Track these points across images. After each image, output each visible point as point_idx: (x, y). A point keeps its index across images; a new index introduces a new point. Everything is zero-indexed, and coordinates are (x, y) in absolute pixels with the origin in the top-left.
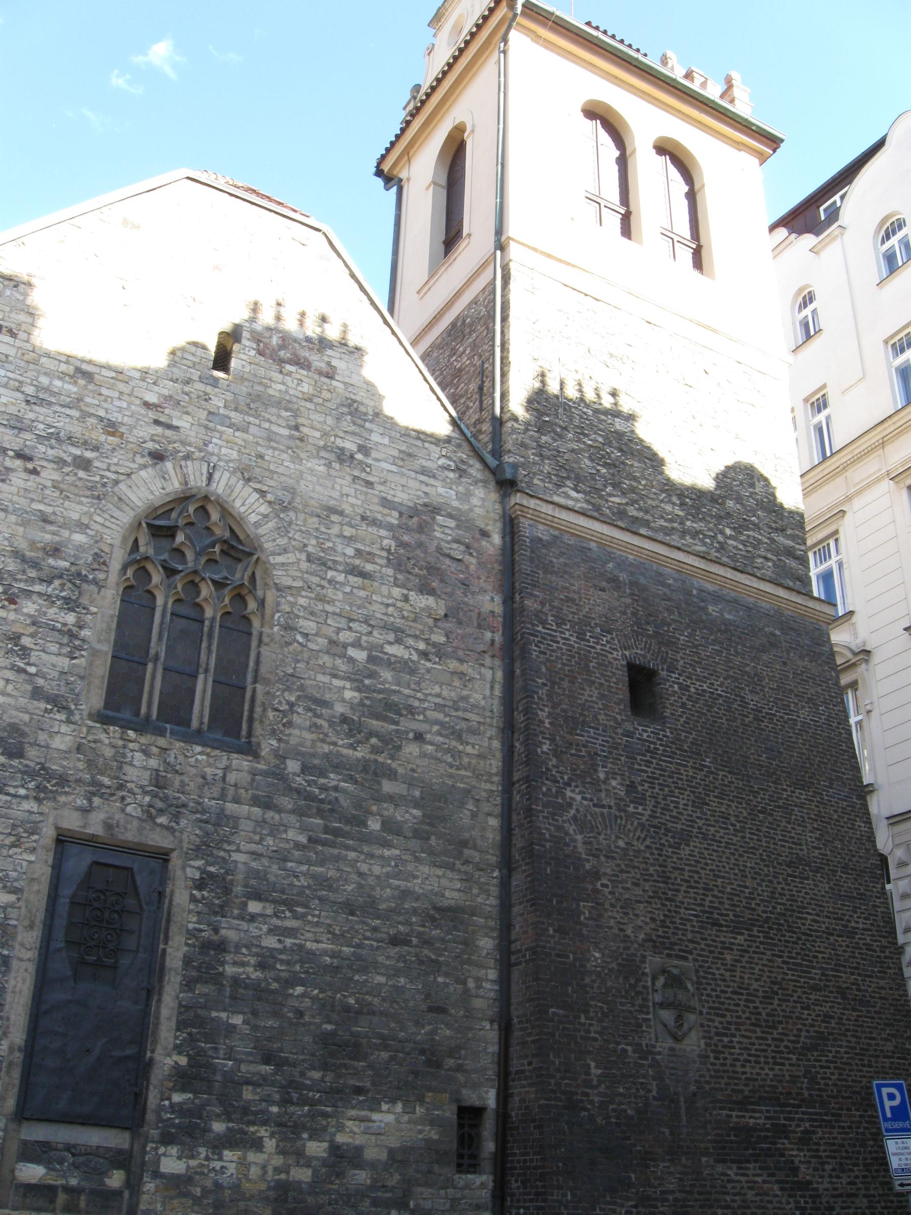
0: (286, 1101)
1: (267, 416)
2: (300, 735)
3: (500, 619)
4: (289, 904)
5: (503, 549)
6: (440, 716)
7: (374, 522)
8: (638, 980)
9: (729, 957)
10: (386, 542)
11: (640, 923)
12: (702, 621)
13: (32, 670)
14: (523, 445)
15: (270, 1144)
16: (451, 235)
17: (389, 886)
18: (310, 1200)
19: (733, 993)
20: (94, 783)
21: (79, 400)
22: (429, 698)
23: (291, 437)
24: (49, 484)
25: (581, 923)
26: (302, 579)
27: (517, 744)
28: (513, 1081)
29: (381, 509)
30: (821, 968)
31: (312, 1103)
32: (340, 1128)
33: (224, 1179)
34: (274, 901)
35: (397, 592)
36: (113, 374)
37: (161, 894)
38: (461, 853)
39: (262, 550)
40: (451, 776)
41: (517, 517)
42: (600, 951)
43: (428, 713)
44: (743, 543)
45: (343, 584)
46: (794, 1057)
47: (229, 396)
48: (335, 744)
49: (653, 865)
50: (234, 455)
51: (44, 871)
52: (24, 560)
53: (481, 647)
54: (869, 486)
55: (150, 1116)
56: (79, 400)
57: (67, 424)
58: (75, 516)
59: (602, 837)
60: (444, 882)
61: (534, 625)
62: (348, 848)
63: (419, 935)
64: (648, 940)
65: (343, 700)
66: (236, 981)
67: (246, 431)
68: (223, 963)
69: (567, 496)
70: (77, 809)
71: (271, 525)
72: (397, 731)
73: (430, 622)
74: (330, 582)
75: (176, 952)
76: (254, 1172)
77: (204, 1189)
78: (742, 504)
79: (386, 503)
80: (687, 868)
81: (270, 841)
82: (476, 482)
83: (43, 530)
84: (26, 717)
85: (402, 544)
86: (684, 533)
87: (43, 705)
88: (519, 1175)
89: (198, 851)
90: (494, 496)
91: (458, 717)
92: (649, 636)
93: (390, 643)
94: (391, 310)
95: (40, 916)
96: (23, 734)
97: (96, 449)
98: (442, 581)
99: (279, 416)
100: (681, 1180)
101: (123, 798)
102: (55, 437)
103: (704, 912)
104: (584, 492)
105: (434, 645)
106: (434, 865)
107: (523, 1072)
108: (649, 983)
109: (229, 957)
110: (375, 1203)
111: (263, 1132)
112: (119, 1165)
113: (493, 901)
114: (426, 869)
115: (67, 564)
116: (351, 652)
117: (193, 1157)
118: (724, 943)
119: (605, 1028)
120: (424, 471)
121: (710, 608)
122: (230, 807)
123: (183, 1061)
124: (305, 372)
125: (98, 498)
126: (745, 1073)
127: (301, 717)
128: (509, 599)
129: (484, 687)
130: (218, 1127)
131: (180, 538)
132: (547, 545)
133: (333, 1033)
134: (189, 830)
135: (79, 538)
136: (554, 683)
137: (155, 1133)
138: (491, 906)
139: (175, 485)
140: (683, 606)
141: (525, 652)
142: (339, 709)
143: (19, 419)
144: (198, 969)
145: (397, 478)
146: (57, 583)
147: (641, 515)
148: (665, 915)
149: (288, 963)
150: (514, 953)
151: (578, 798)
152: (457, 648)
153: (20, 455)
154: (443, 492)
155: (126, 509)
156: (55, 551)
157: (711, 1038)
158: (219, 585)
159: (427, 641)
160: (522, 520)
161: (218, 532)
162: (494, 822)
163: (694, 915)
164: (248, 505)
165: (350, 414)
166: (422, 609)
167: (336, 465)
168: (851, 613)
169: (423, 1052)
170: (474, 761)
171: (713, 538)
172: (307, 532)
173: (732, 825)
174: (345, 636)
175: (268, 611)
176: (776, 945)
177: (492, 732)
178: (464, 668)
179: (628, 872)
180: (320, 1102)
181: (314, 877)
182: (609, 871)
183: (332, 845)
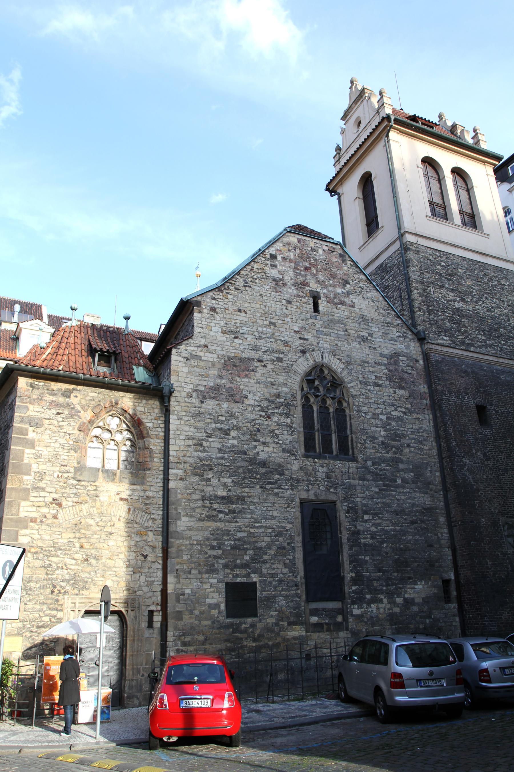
0: (387, 585)
2: (370, 452)
4: (377, 514)
6: (414, 436)
7: (379, 364)
8: (498, 528)
10: (384, 371)
13: (281, 442)
14: (424, 321)
15: (385, 601)
16: (372, 224)
17: (408, 503)
18: (400, 618)
20: (308, 480)
21: (273, 334)
23: (345, 335)
24: (271, 370)
32: (406, 592)
33: (373, 614)
34: (372, 514)
35: (391, 390)
37: (336, 517)
38: (429, 487)
39: (345, 382)
40: (421, 458)
42: (484, 518)
44: (509, 346)
45: (373, 391)
47: (321, 322)
48: (381, 453)
50: (328, 346)
51: (298, 515)
52: (269, 401)
53: (423, 407)
55: (347, 595)
56: (273, 334)
57: (272, 346)
58: (282, 381)
60: (425, 499)
62: (392, 491)
63: (420, 519)
64: (499, 512)
65: (381, 436)
66: (365, 544)
67: (330, 336)
68: (360, 539)
69: (443, 339)
70: (305, 491)
71: (346, 372)
73: (404, 400)
74: (369, 390)
75: (345, 536)
76: (382, 610)
77: (367, 619)
79: (382, 355)
81: (367, 492)
83: (273, 388)
84: (282, 460)
85: (390, 371)
86: (486, 346)
87: (287, 455)
89: (345, 499)
90: (418, 345)
92: (481, 393)
95: (301, 531)
96: (283, 466)
97: (283, 353)
99: (339, 327)
101: (318, 484)
102: (268, 351)
104: (448, 336)
105: (408, 409)
106: (421, 493)
109: (361, 536)
110: (421, 617)
111: (382, 597)
112: (340, 614)
113: (442, 503)
114: (418, 495)
116: (381, 417)
117: (362, 608)
120: (392, 339)
122: (352, 482)
123: (353, 575)
125: (288, 372)
128: (430, 387)
129: (426, 422)
130: (368, 596)
131: (317, 383)
132: (441, 362)
133: (398, 559)
134: (341, 494)
135: (285, 389)
137: (349, 601)
139: (311, 362)
141: (440, 407)
142: (381, 439)
143: (255, 346)
144: (352, 542)
145: (383, 344)
146: (281, 408)
149: (380, 535)
151: (468, 461)
153: (259, 361)
154: (400, 347)
156: (278, 396)
158: (333, 399)
159: (405, 408)
161: (328, 377)
162: (438, 474)
164: (337, 365)
167: (362, 343)
169: (428, 562)
171: (498, 346)
172: (358, 372)
174: (378, 411)
175: (351, 406)
177: (432, 439)
178: (419, 416)
180: (398, 584)
181: (383, 503)
183: (387, 490)
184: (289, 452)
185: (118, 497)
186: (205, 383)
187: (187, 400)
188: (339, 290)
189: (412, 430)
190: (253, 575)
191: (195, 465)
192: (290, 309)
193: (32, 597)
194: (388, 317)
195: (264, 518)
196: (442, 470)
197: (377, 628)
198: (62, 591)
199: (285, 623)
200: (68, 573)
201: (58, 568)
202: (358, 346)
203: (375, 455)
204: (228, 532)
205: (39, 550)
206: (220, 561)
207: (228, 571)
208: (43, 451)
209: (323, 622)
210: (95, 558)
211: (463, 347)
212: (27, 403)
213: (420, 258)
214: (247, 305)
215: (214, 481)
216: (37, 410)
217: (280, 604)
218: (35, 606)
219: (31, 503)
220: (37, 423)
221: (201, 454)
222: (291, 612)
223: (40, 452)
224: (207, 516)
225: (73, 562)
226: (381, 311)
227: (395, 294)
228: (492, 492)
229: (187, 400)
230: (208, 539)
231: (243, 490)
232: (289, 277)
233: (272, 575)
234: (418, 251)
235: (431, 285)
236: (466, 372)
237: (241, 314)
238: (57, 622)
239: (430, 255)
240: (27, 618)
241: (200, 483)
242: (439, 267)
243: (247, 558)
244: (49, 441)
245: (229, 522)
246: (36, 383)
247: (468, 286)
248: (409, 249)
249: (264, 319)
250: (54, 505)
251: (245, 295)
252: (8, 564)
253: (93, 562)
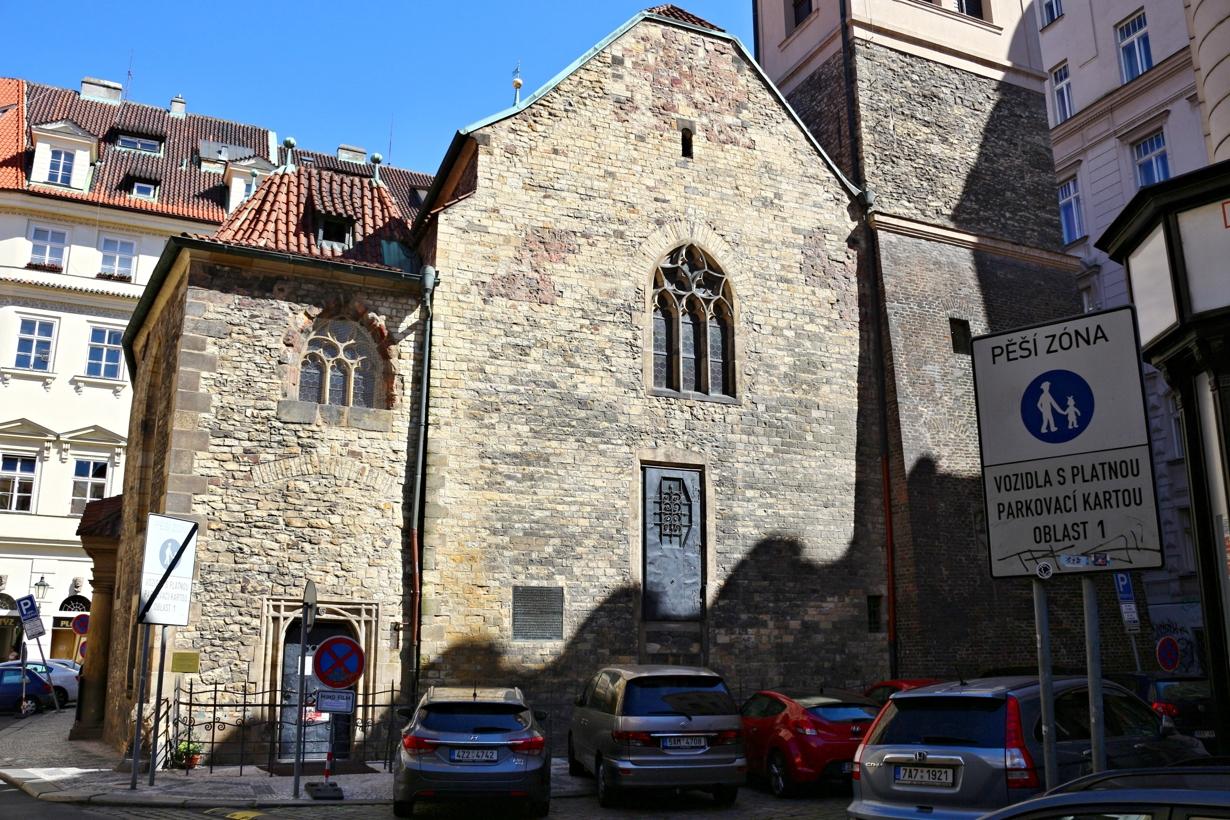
0: (777, 600)
1: (719, 183)
6: (840, 366)
8: (966, 518)
13: (613, 369)
15: (771, 624)
22: (834, 356)
24: (603, 251)
26: (753, 290)
27: (887, 379)
29: (793, 235)
31: (790, 600)
32: (806, 613)
35: (808, 289)
36: (627, 171)
43: (833, 365)
44: (1017, 221)
48: (783, 391)
54: (1100, 142)
58: (621, 270)
62: (795, 453)
67: (708, 196)
71: (731, 256)
72: (817, 379)
76: (764, 639)
78: (1016, 194)
79: (795, 230)
81: (753, 454)
83: (605, 281)
87: (623, 390)
91: (850, 365)
92: (962, 298)
93: (807, 323)
94: (757, 59)
104: (914, 202)
108: (973, 519)
109: (739, 523)
112: (696, 641)
113: (879, 476)
115: (622, 302)
116: (787, 333)
117: (732, 634)
121: (999, 273)
124: (736, 148)
127: (762, 377)
130: (744, 617)
135: (626, 283)
137: (712, 622)
139: (672, 243)
142: (783, 369)
153: (584, 235)
155: (649, 260)
156: (613, 294)
159: (829, 319)
162: (875, 428)
164: (714, 246)
165: (767, 172)
166: (823, 298)
167: (763, 210)
168: (1086, 238)
169: (846, 567)
171: (999, 220)
174: (782, 323)
180: (795, 599)
184: (625, 386)
185: (344, 453)
186: (492, 271)
187: (461, 297)
188: (729, 119)
189: (838, 356)
190: (557, 577)
191: (470, 402)
192: (643, 150)
193: (213, 595)
195: (581, 490)
197: (755, 665)
198: (259, 588)
199: (606, 652)
200: (268, 563)
201: (253, 554)
202: (756, 213)
203: (771, 395)
204: (520, 510)
205: (222, 526)
206: (506, 553)
207: (519, 568)
208: (229, 376)
209: (668, 651)
210: (310, 542)
211: (938, 221)
212: (203, 299)
214: (568, 141)
215: (501, 429)
216: (220, 310)
217: (599, 622)
218: (217, 608)
219: (211, 455)
220: (219, 332)
221: (481, 386)
222: (616, 636)
223: (225, 377)
224: (486, 483)
225: (276, 546)
226: (800, 157)
227: (831, 127)
229: (461, 297)
230: (487, 519)
231: (548, 443)
232: (644, 95)
233: (590, 578)
237: (558, 157)
238: (251, 634)
240: (206, 624)
241: (478, 430)
242: (908, 83)
243: (549, 549)
244: (239, 359)
245: (522, 493)
246: (218, 267)
249: (596, 165)
250: (246, 459)
251: (566, 125)
252: (170, 544)
253: (307, 547)
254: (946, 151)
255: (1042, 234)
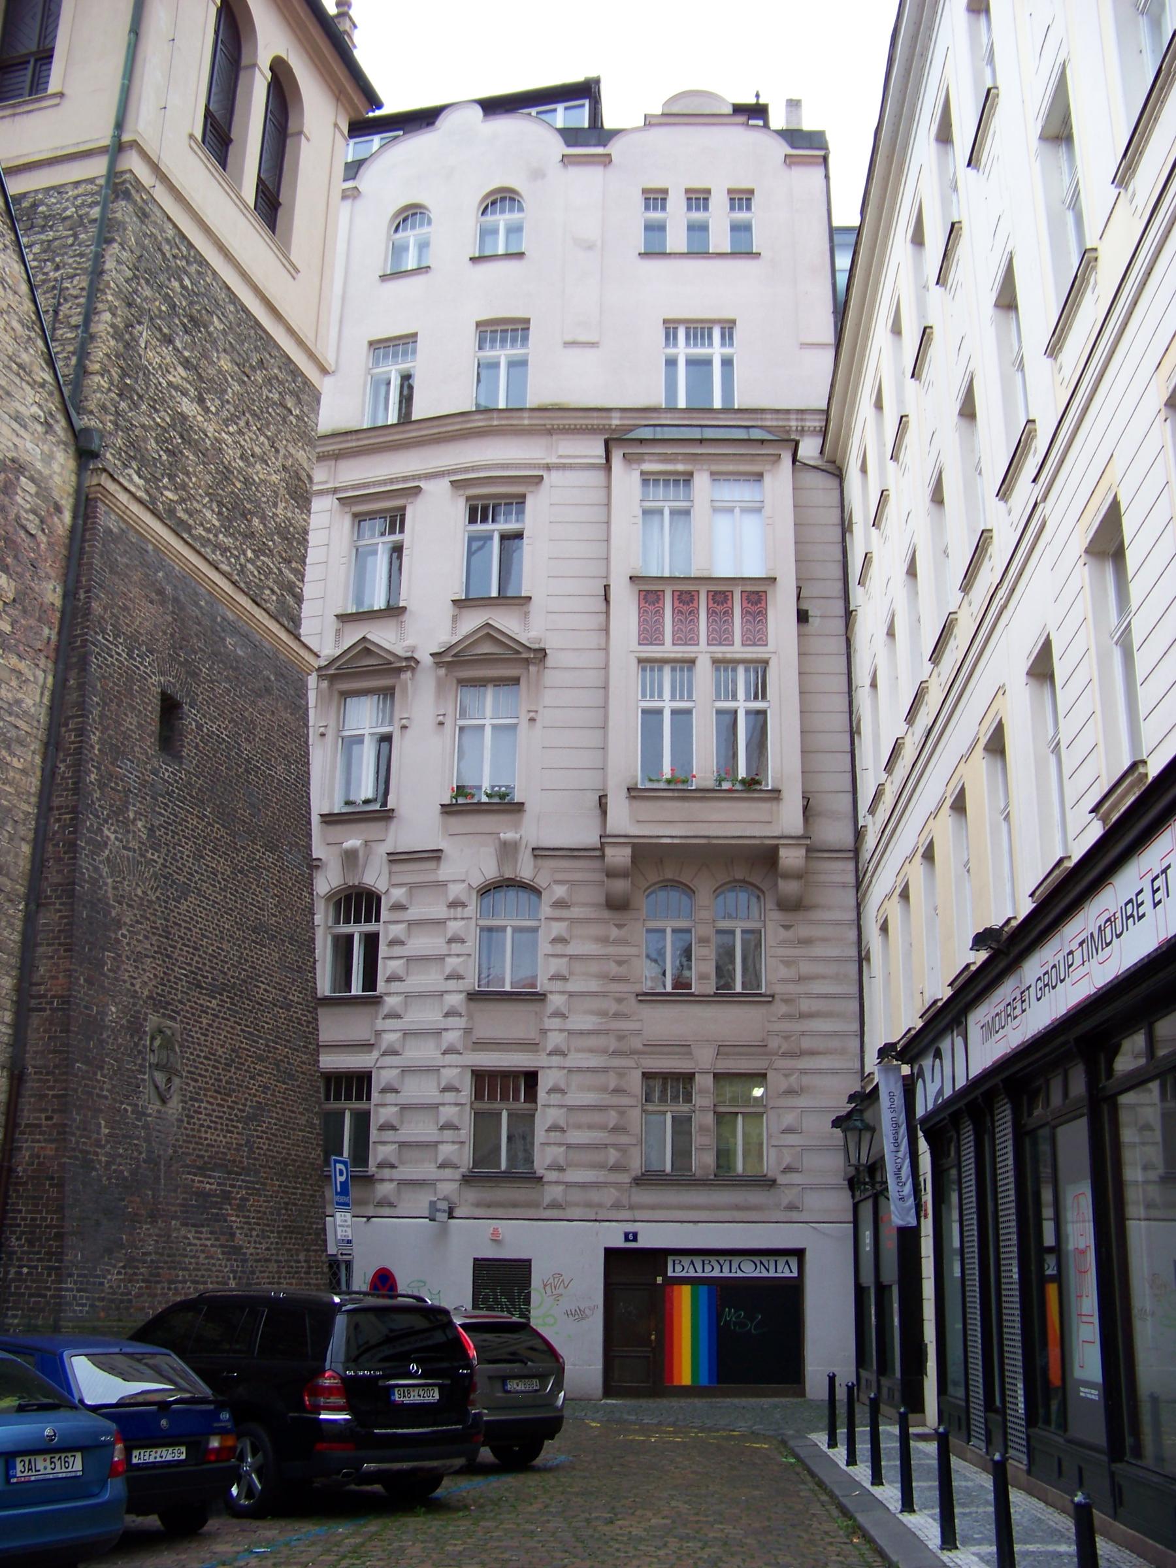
3: (58, 615)
5: (73, 530)
8: (141, 1039)
9: (205, 1021)
11: (146, 979)
12: (220, 654)
14: (104, 408)
19: (206, 1058)
25: (104, 975)
27: (62, 767)
28: (23, 1133)
30: (266, 1039)
41: (96, 499)
42: (116, 1005)
44: (258, 568)
46: (240, 1125)
49: (160, 918)
59: (126, 883)
61: (96, 633)
64: (150, 997)
78: (265, 525)
80: (183, 924)
82: (60, 442)
86: (217, 546)
88: (23, 1233)
90: (72, 464)
98: (16, 557)
100: (157, 1241)
103: (192, 972)
104: (147, 480)
107: (39, 1126)
113: (16, 937)
118: (202, 1005)
119: (114, 1086)
120: (17, 418)
126: (206, 1139)
128: (69, 595)
136: (105, 704)
138: (14, 942)
140: (209, 633)
147: (184, 517)
148: (164, 973)
150: (32, 997)
152: (19, 641)
157: (186, 1103)
160: (99, 504)
162: (26, 849)
163: (185, 975)
170: (18, 776)
171: (237, 558)
173: (220, 883)
176: (237, 1012)
178: (22, 666)
179: (141, 923)
182: (128, 920)
194: (26, 349)
196: (40, 840)
213: (145, 235)
226: (15, 324)
228: (146, 937)
234: (146, 215)
235: (146, 319)
236: (161, 592)
239: (168, 241)
242: (176, 284)
247: (220, 371)
248: (127, 195)
254: (200, 418)
255: (281, 602)
